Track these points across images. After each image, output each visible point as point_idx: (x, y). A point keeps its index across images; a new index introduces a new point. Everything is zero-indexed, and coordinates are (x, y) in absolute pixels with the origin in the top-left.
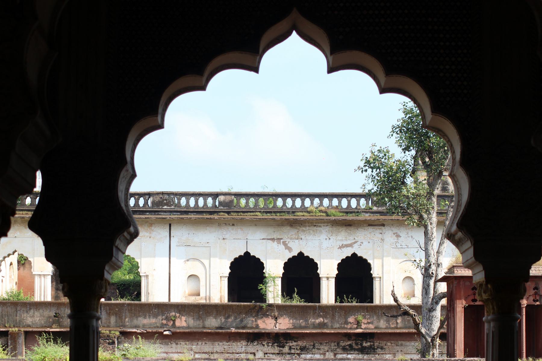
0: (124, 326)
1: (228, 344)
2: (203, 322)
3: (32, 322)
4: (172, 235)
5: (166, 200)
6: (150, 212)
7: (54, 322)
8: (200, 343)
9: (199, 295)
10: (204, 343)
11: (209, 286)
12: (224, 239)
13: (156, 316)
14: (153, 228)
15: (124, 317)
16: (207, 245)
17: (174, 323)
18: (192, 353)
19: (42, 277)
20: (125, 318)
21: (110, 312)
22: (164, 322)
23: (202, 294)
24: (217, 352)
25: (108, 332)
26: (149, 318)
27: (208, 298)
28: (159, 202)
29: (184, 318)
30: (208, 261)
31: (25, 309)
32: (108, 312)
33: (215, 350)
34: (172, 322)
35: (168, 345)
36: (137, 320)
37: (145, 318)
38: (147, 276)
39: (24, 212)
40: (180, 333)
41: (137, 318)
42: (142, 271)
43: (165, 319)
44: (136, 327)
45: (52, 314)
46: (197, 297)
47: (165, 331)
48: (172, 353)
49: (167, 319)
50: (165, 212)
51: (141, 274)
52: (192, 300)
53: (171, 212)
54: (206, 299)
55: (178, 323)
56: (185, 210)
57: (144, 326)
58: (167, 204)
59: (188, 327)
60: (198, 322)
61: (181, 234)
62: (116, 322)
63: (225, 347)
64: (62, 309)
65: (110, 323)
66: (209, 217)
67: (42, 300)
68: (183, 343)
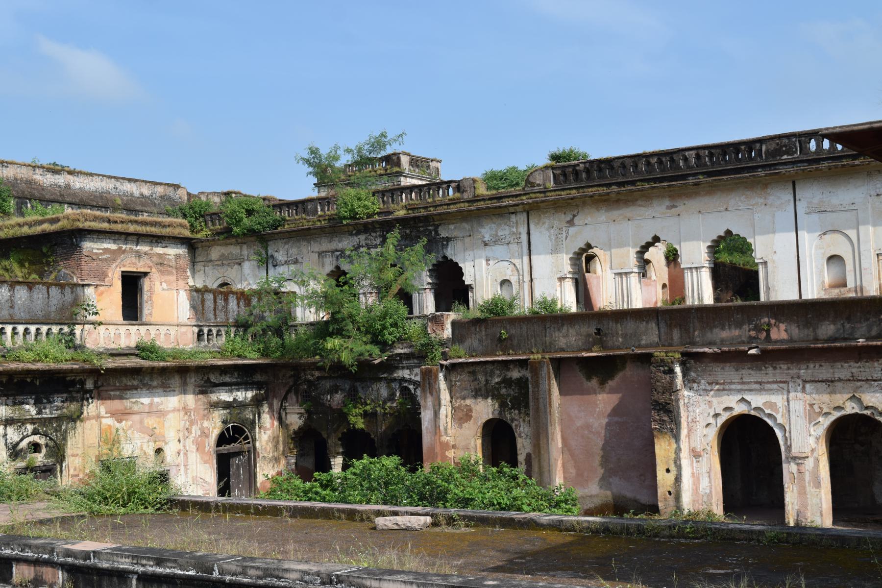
0: (693, 344)
1: (857, 365)
2: (814, 330)
3: (566, 344)
4: (797, 198)
5: (785, 146)
6: (763, 167)
7: (594, 344)
8: (812, 366)
9: (845, 285)
10: (817, 366)
11: (859, 271)
12: (878, 195)
13: (739, 325)
14: (769, 191)
15: (691, 330)
16: (852, 207)
17: (768, 335)
18: (800, 382)
19: (624, 278)
20: (694, 331)
21: (671, 323)
22: (753, 333)
23: (850, 284)
24: (840, 380)
25: (663, 354)
26: (730, 328)
27: (858, 289)
28: (776, 150)
29: (783, 326)
30: (855, 231)
31: (556, 326)
32: (669, 322)
33: (837, 376)
34: (765, 334)
35: (761, 370)
36: (712, 332)
37: (723, 329)
38: (765, 263)
39: (594, 189)
40: (773, 351)
41: (711, 329)
42: (759, 254)
43: (753, 330)
44: (710, 344)
45: (593, 330)
46: (843, 289)
47: (750, 349)
48: (768, 382)
49: (758, 329)
50: (785, 164)
51: (756, 261)
52: (835, 294)
53: (793, 163)
54: (856, 291)
55: (774, 335)
56: (815, 157)
57: (723, 342)
58: (787, 153)
59: (791, 340)
60: (806, 332)
61: (811, 195)
62: (681, 337)
63: (854, 370)
64: (605, 322)
65: (672, 339)
66: (851, 162)
67: (626, 307)
68: (784, 367)
